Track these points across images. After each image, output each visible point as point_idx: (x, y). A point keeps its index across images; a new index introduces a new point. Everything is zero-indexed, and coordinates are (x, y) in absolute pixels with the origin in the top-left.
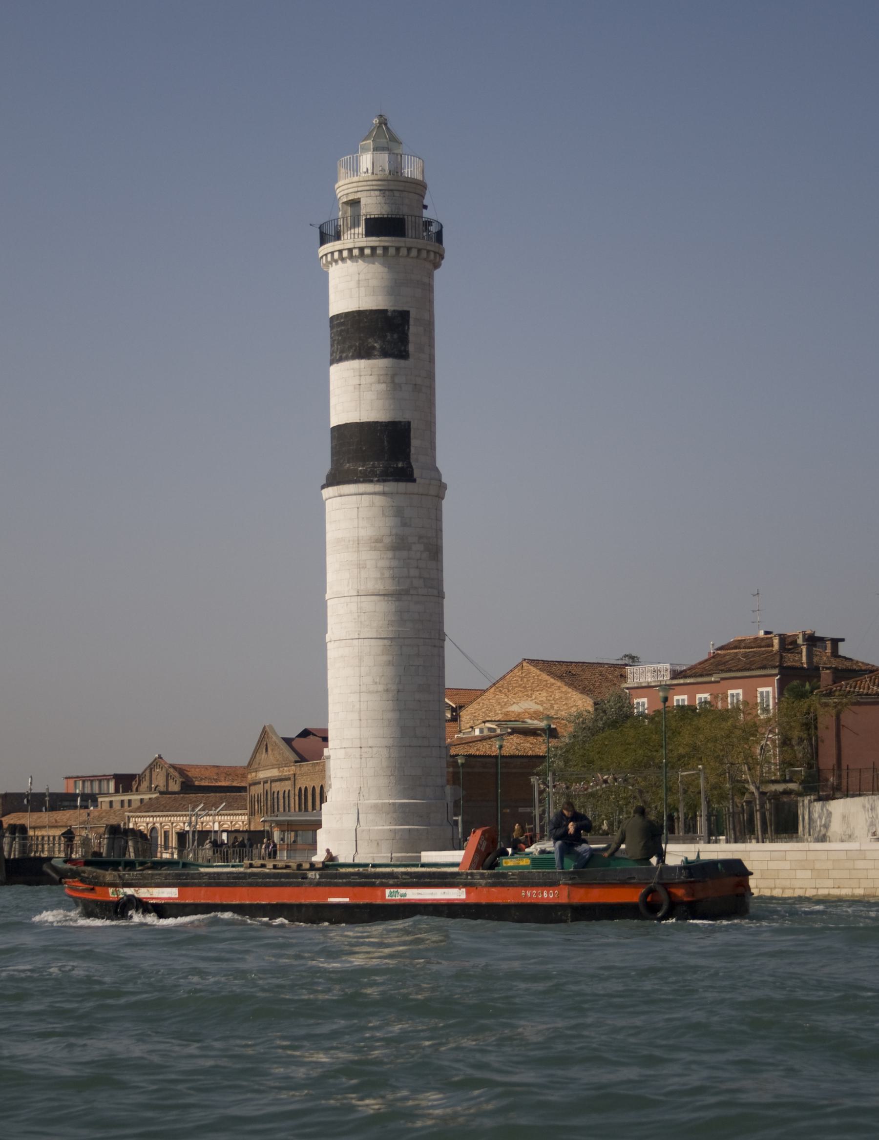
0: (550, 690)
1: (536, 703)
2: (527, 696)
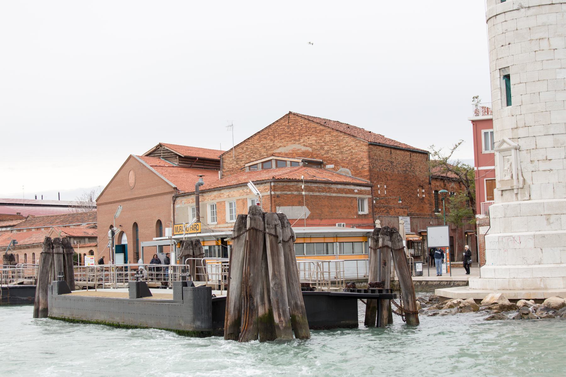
0: (319, 135)
1: (304, 145)
2: (295, 140)
